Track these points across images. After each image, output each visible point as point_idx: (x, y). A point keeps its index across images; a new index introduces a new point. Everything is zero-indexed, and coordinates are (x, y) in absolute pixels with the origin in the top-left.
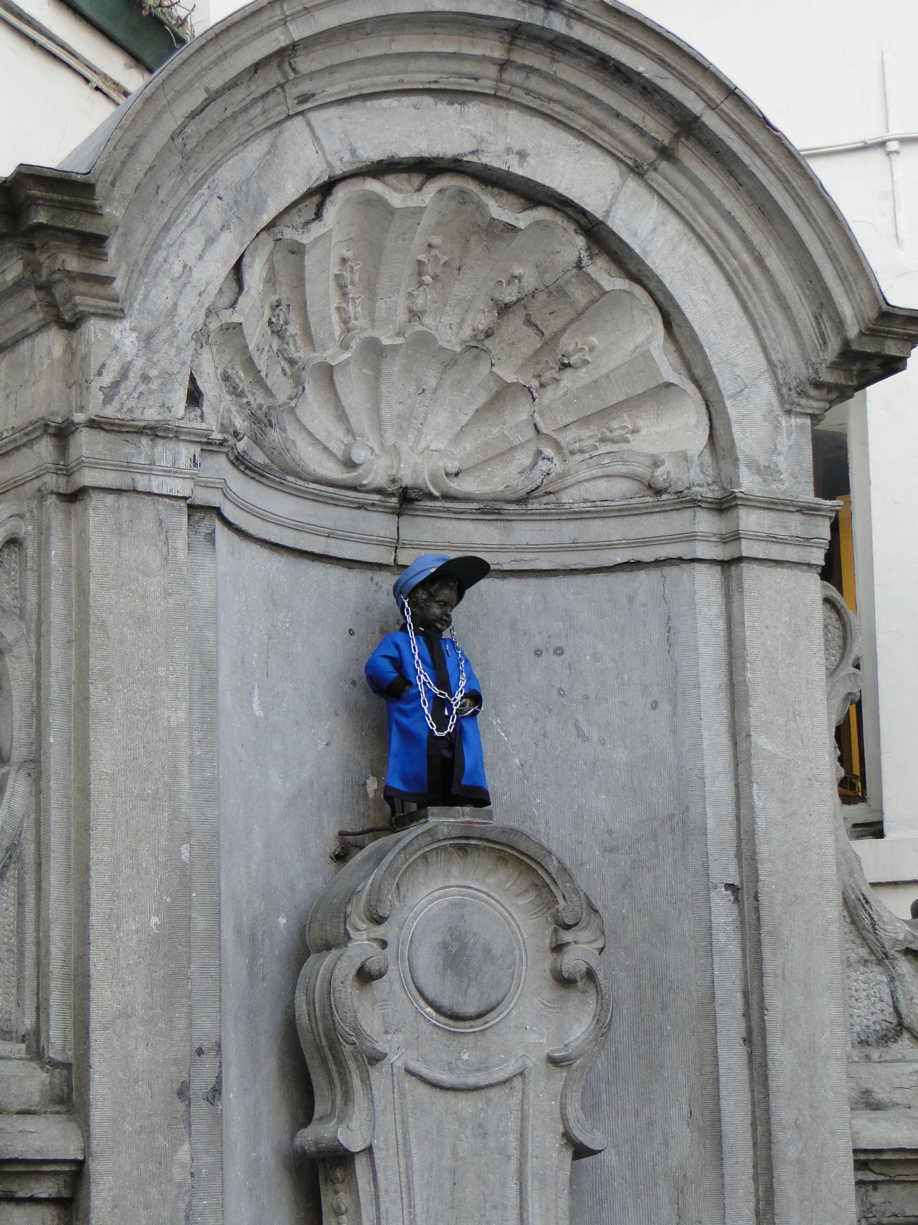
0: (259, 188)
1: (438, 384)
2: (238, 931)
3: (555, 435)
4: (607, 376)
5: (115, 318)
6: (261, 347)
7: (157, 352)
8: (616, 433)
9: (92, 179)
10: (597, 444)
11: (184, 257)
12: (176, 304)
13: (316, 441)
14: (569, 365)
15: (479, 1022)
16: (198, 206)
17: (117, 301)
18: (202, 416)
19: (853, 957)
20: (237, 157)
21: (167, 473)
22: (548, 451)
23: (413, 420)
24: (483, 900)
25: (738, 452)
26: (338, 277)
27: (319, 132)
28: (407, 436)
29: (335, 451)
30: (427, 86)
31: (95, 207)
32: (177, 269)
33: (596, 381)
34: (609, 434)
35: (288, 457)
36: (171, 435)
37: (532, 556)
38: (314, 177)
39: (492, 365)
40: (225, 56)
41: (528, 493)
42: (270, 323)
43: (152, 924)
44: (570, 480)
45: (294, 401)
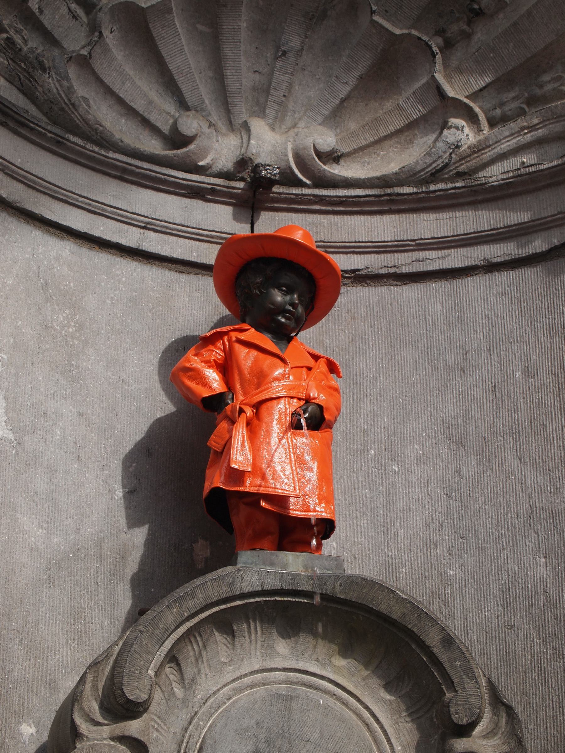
1: (303, 43)
3: (466, 101)
4: (529, 13)
8: (549, 87)
10: (524, 106)
13: (130, 112)
14: (479, 13)
23: (272, 91)
24: (327, 692)
28: (264, 112)
29: (158, 124)
33: (515, 24)
34: (538, 92)
37: (440, 253)
39: (373, 12)
41: (433, 175)
44: (488, 154)
45: (88, 49)
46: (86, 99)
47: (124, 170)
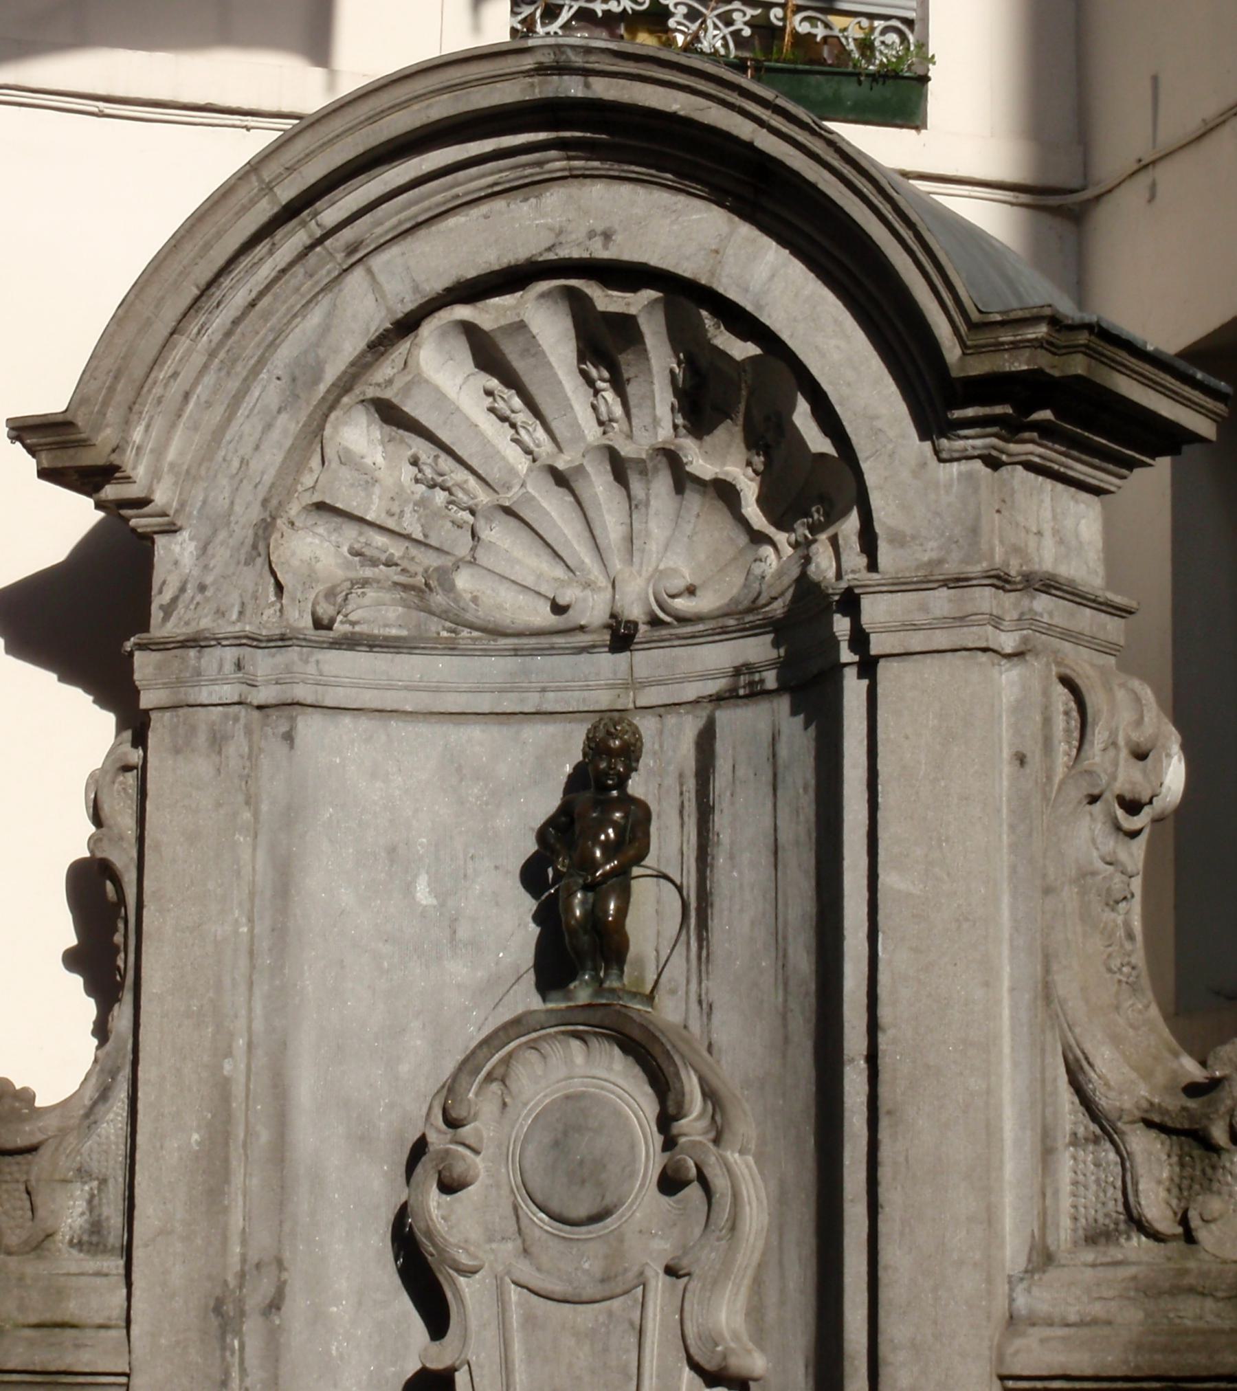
0: (317, 356)
2: (362, 1140)
5: (175, 531)
6: (396, 509)
7: (213, 556)
9: (69, 417)
11: (241, 452)
12: (232, 503)
15: (568, 1228)
16: (257, 394)
17: (166, 515)
18: (281, 610)
19: (1081, 1131)
20: (297, 330)
21: (214, 682)
22: (768, 550)
25: (875, 524)
26: (492, 410)
27: (381, 278)
30: (490, 191)
31: (84, 440)
32: (236, 463)
35: (469, 616)
36: (213, 643)
38: (373, 329)
40: (208, 246)
42: (417, 481)
43: (193, 1140)
46: (475, 600)
47: (515, 650)
